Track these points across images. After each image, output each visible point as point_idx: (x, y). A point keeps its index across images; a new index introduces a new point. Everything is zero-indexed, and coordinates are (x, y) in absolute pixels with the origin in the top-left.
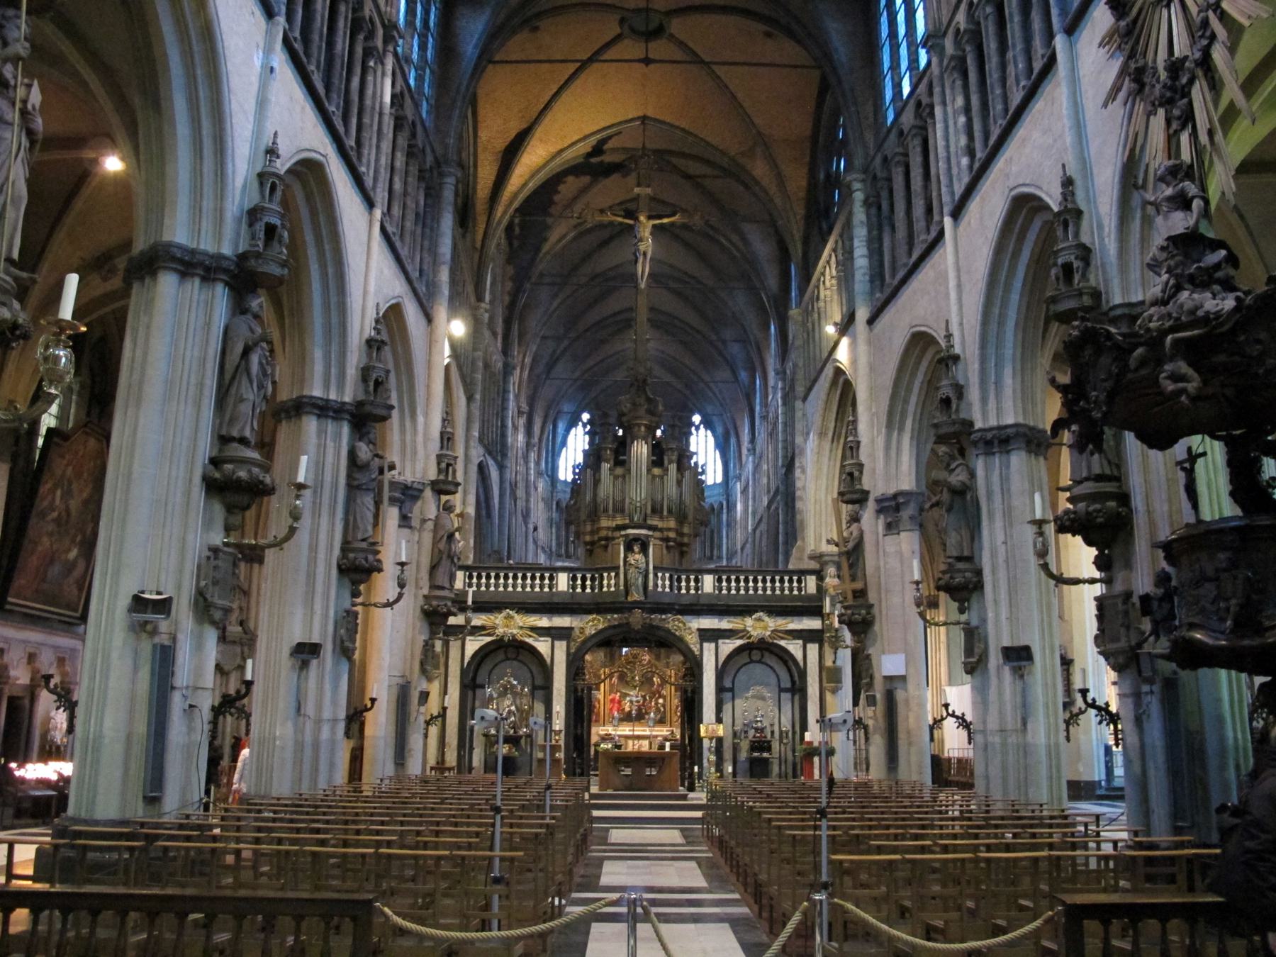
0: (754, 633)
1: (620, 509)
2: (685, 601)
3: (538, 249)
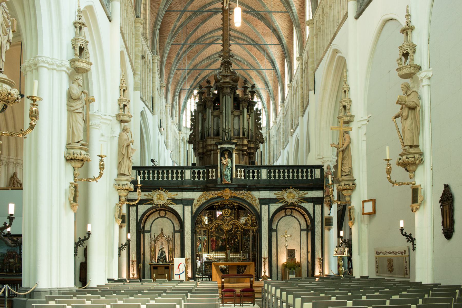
1: (217, 134)
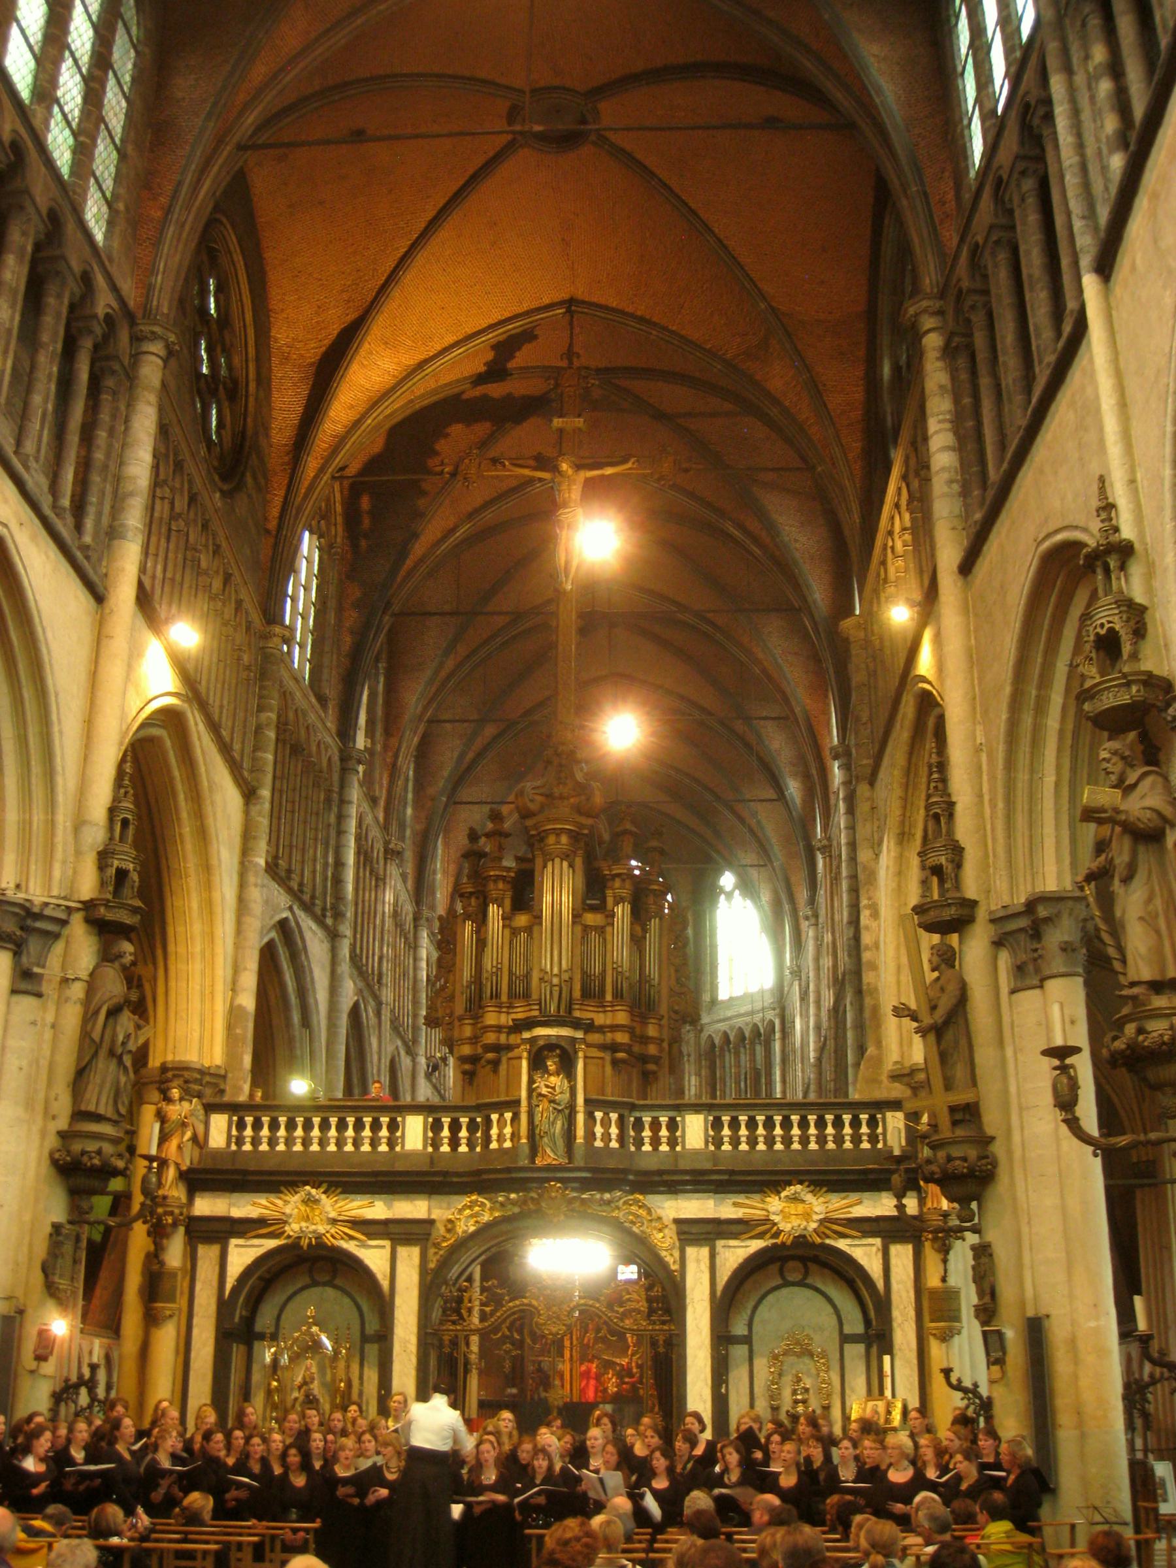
0: (785, 1226)
1: (521, 992)
2: (651, 1164)
3: (403, 554)
